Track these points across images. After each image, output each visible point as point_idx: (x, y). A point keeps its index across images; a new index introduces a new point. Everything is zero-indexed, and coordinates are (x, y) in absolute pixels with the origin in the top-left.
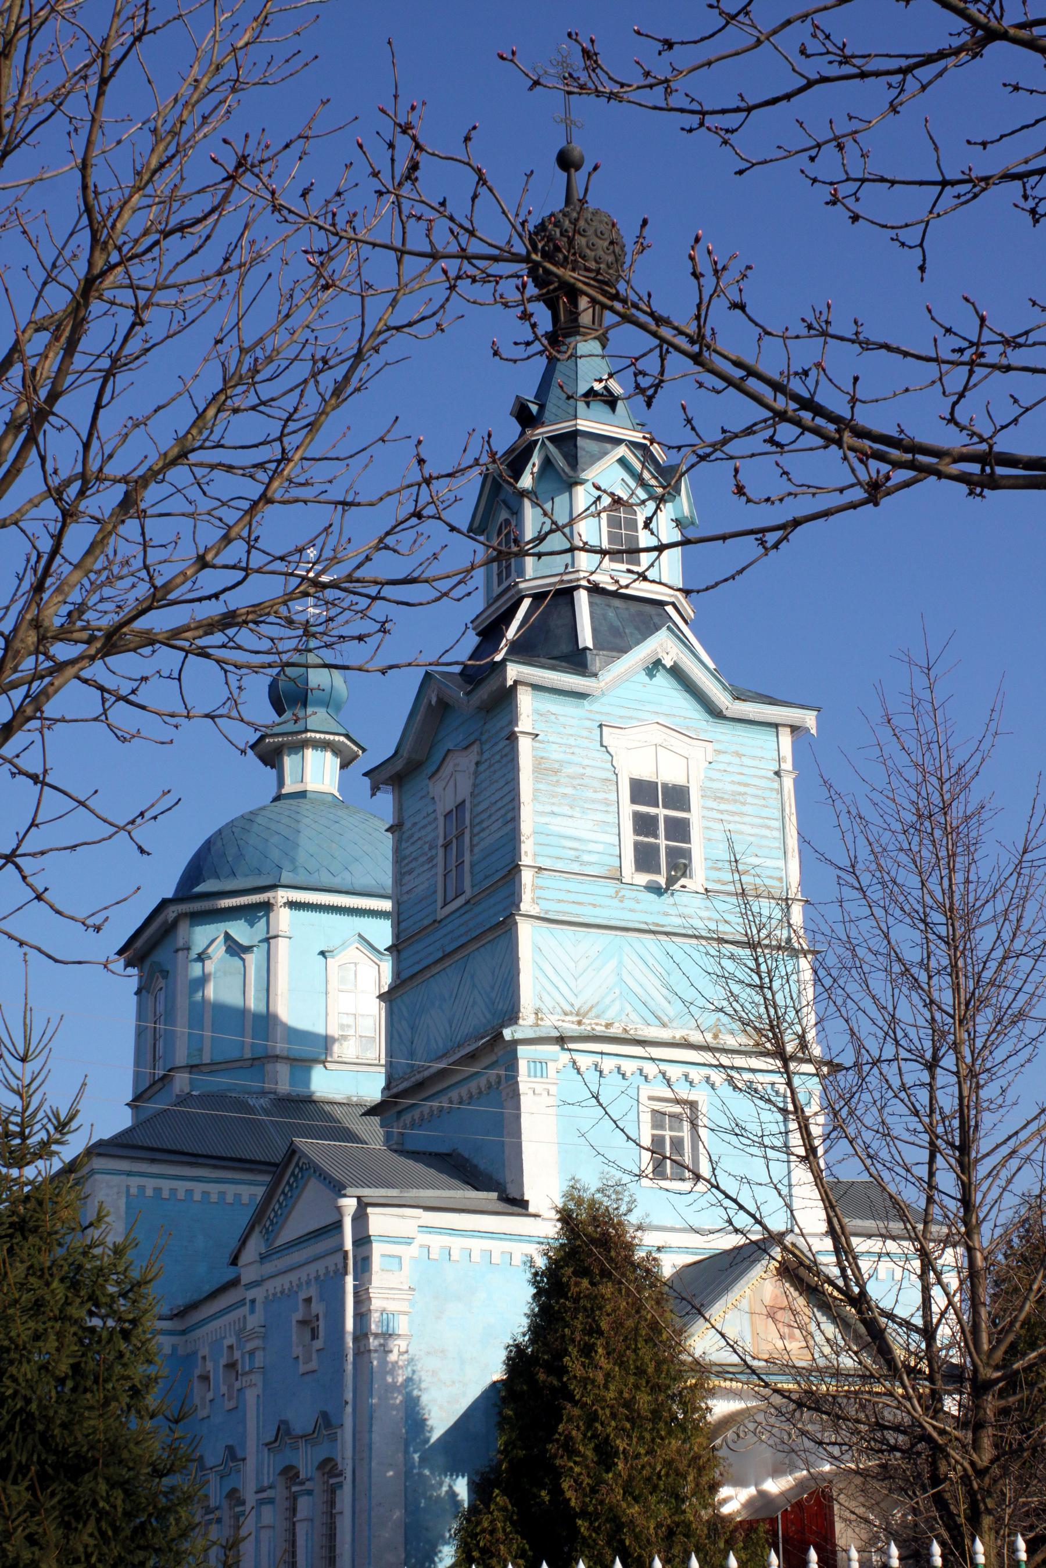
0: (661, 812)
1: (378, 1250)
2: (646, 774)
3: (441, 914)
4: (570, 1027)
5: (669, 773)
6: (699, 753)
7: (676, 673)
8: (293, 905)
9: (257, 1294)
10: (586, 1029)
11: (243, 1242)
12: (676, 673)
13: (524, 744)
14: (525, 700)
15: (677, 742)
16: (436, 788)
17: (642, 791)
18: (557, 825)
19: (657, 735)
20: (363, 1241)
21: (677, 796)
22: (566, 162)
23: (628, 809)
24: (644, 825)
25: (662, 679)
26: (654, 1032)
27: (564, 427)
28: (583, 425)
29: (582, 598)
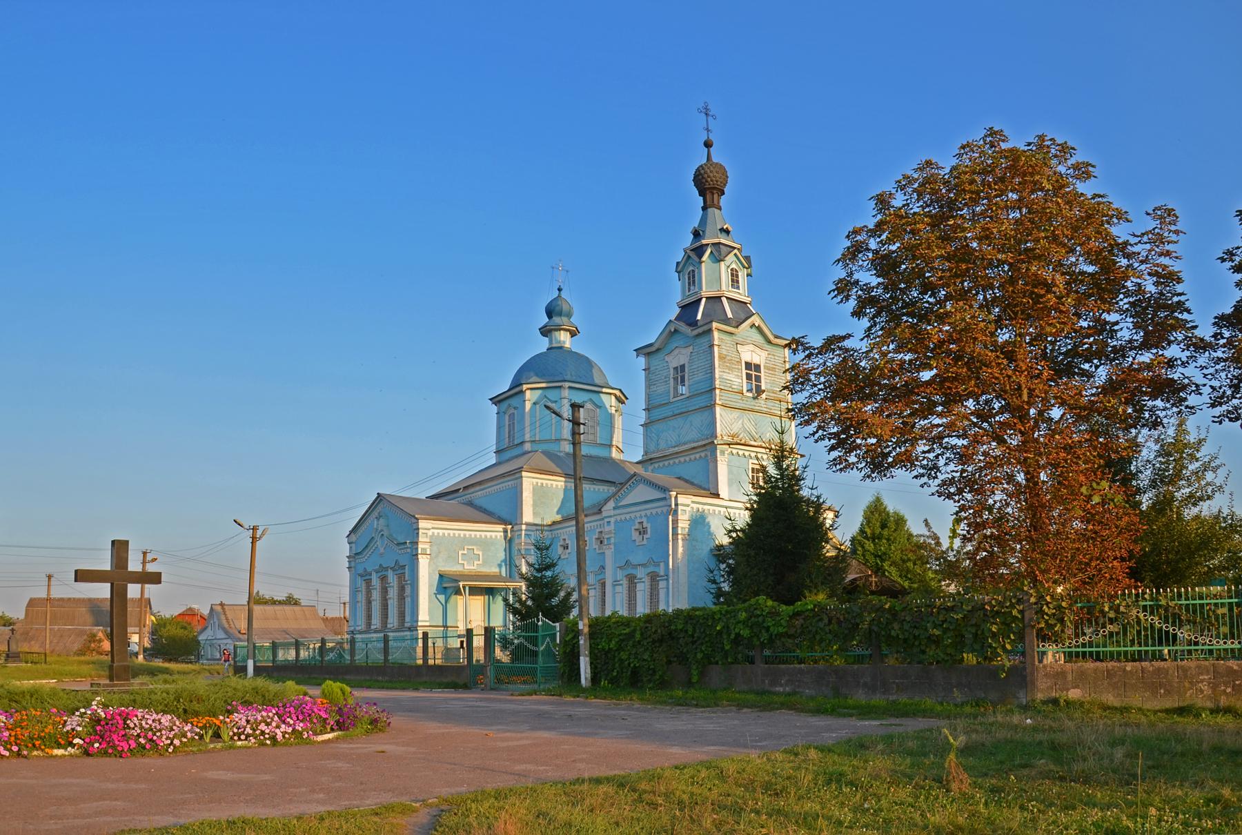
0: (754, 373)
1: (680, 508)
2: (749, 360)
4: (730, 439)
5: (756, 360)
6: (764, 354)
7: (759, 329)
9: (612, 520)
10: (736, 440)
11: (607, 501)
12: (759, 329)
13: (716, 348)
14: (716, 334)
15: (757, 350)
18: (725, 376)
19: (751, 347)
20: (676, 505)
21: (757, 368)
23: (744, 372)
24: (749, 377)
25: (754, 330)
26: (753, 443)
27: (716, 241)
28: (723, 241)
29: (724, 299)
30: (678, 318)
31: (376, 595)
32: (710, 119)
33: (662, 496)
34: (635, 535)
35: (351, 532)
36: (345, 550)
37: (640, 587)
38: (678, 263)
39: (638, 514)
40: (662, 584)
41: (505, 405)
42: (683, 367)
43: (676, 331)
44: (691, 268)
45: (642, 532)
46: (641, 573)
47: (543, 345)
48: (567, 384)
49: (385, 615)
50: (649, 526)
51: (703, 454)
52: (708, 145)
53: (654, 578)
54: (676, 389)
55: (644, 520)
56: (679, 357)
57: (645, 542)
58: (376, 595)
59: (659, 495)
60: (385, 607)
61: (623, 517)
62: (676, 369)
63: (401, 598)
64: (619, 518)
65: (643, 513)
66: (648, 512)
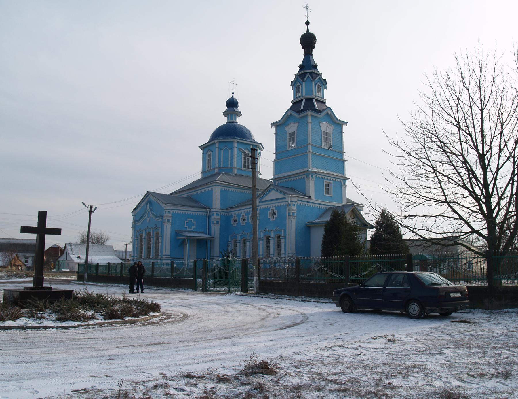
3: (288, 149)
5: (328, 131)
8: (238, 142)
16: (287, 128)
17: (325, 133)
22: (307, 23)
30: (291, 108)
31: (144, 242)
32: (308, 11)
33: (283, 196)
34: (270, 217)
35: (134, 210)
36: (131, 218)
37: (272, 241)
38: (292, 82)
39: (271, 205)
40: (283, 240)
41: (207, 149)
42: (293, 133)
43: (291, 115)
44: (298, 84)
45: (273, 214)
46: (272, 235)
47: (224, 121)
48: (236, 140)
49: (149, 252)
50: (276, 211)
51: (303, 177)
52: (307, 23)
53: (279, 238)
54: (289, 144)
55: (274, 208)
56: (292, 128)
57: (274, 219)
58: (144, 242)
59: (283, 196)
60: (149, 247)
61: (264, 207)
62: (290, 134)
63: (157, 243)
64: (262, 207)
65: (274, 205)
66: (276, 205)
